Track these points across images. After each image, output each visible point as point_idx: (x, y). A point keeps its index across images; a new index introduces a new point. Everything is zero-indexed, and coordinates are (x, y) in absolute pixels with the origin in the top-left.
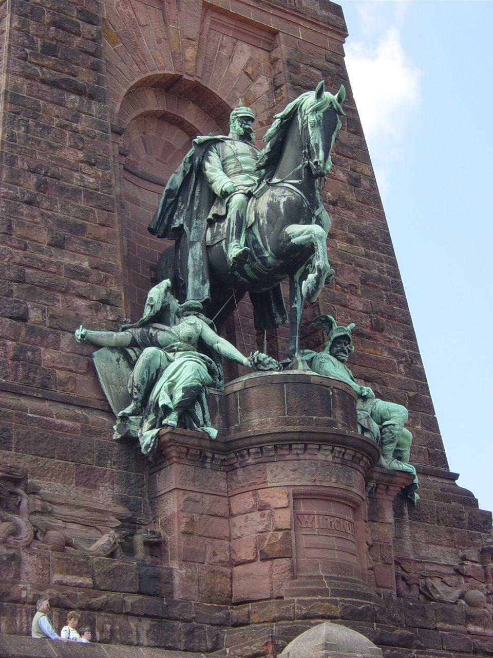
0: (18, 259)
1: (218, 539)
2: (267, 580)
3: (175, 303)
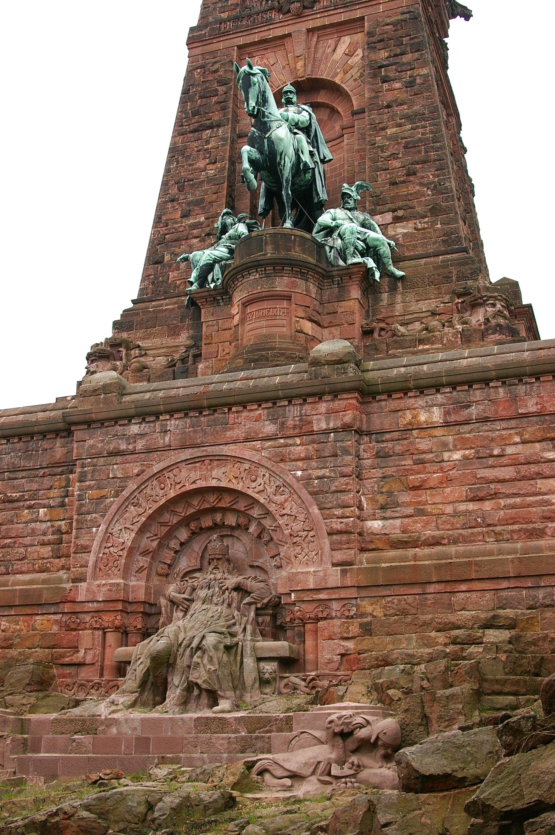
0: (162, 233)
3: (229, 220)
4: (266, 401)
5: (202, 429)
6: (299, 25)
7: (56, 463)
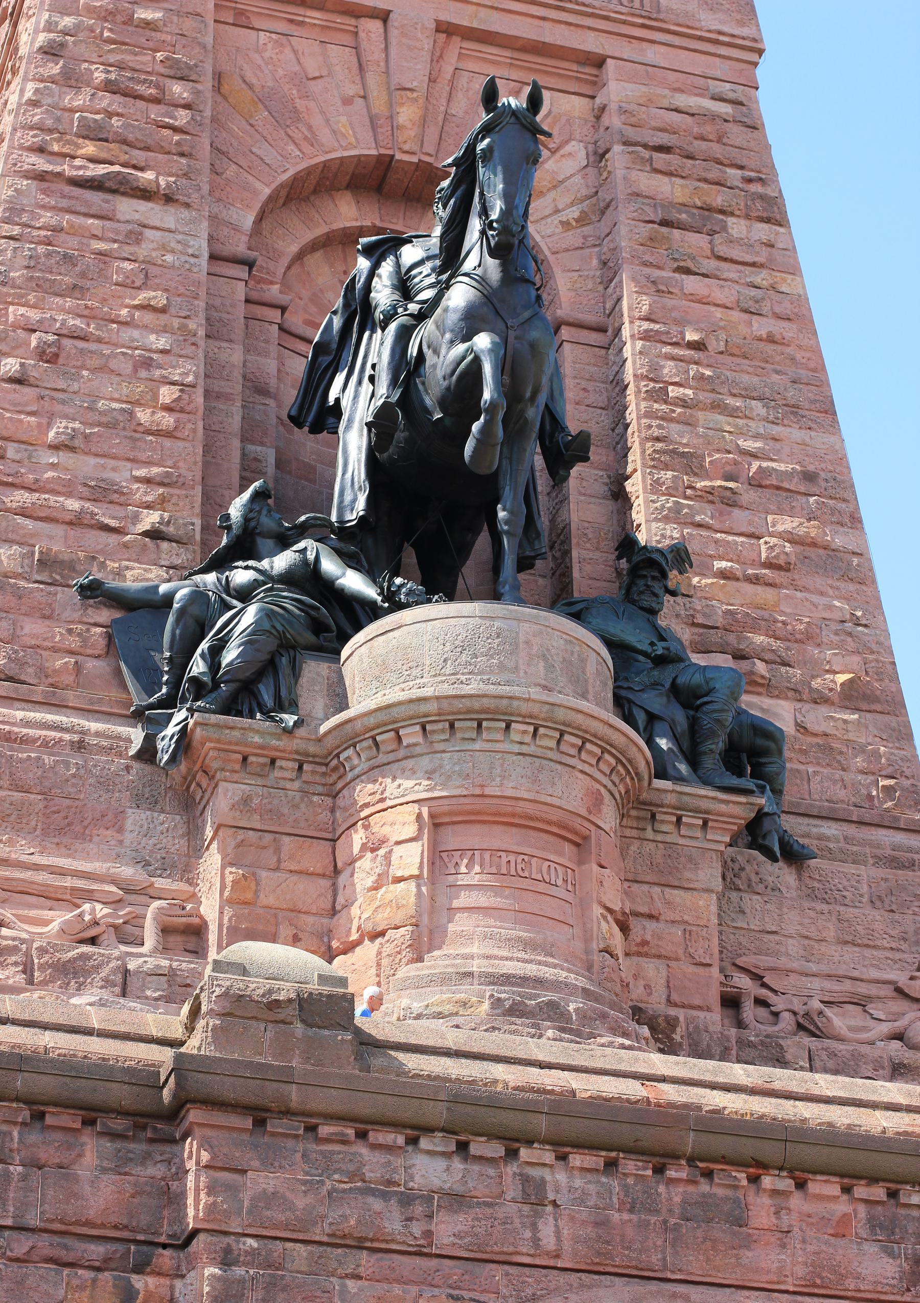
1: (305, 913)
2: (373, 971)
4: (873, 1180)
5: (665, 1222)
7: (88, 1223)
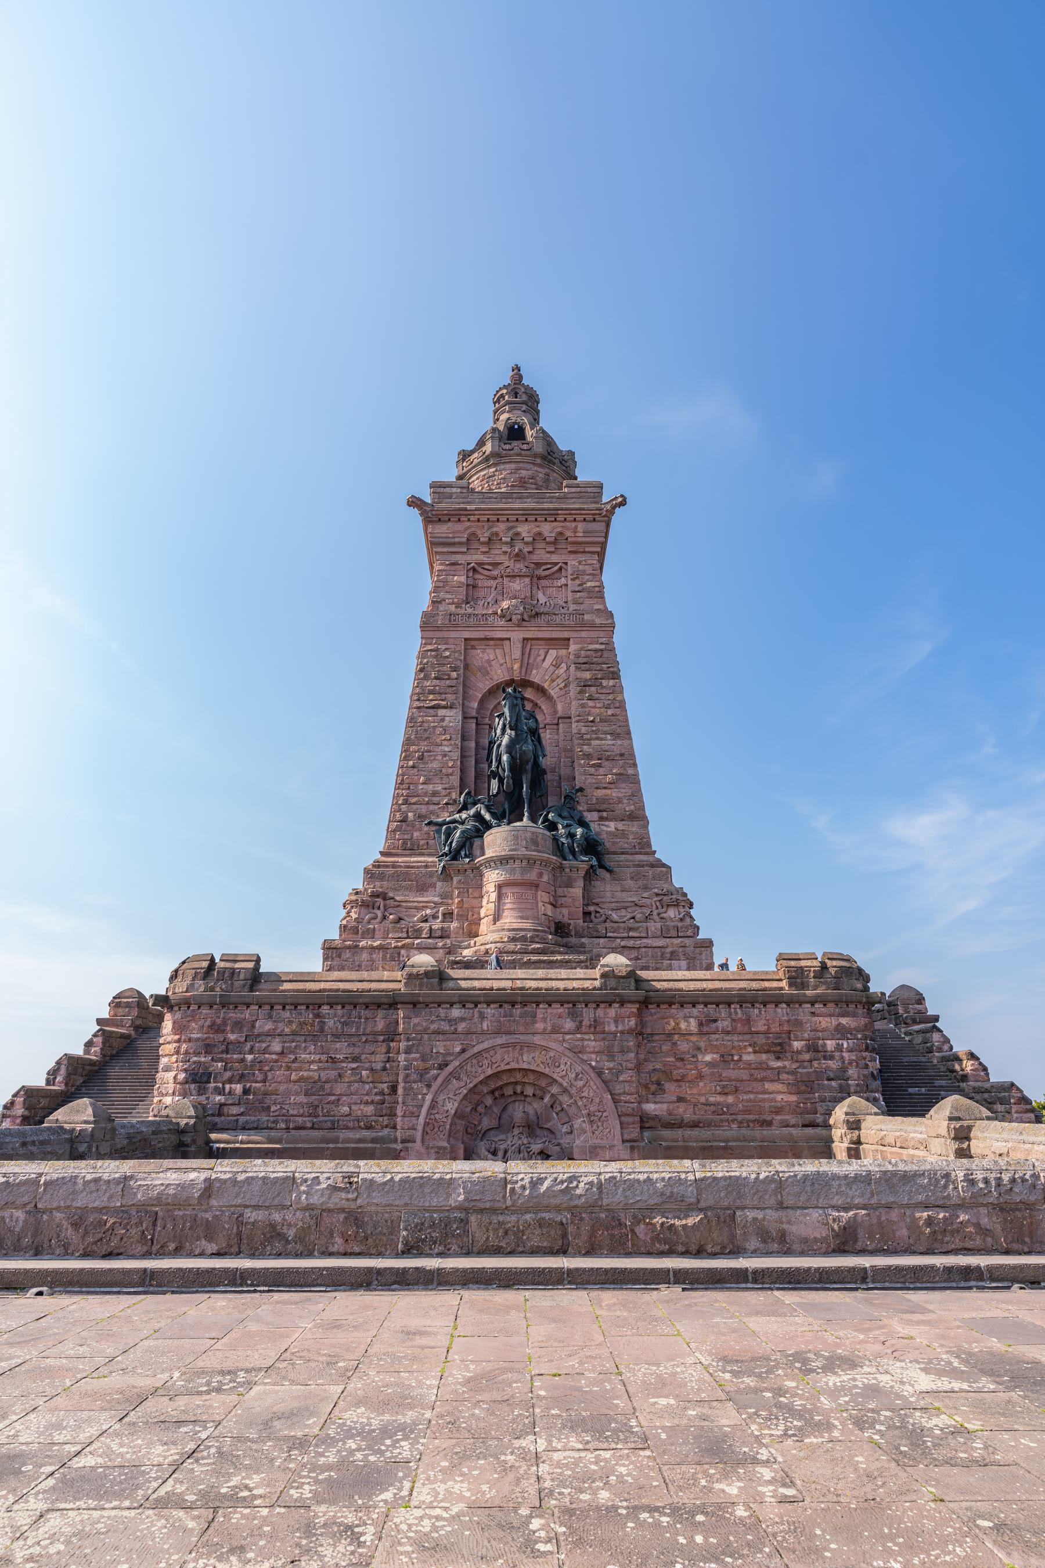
4: (568, 1003)
6: (517, 633)
